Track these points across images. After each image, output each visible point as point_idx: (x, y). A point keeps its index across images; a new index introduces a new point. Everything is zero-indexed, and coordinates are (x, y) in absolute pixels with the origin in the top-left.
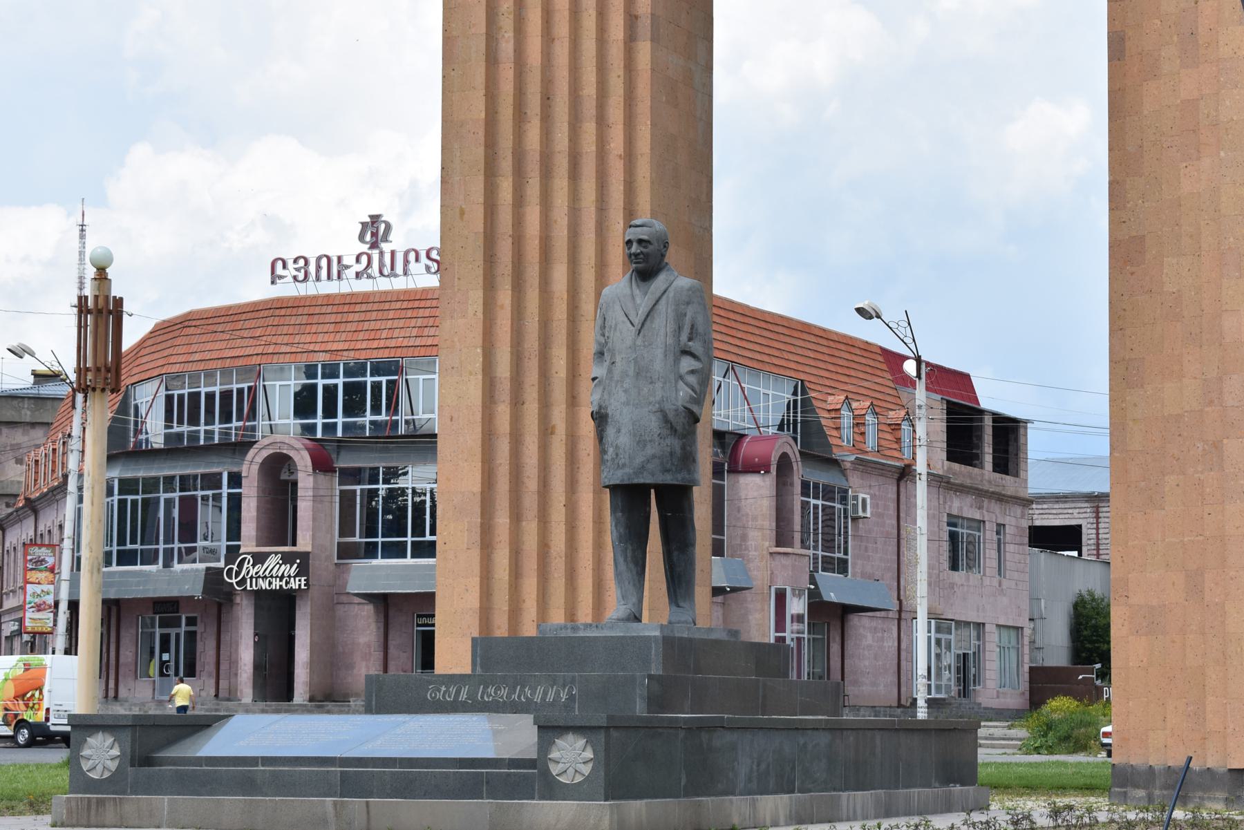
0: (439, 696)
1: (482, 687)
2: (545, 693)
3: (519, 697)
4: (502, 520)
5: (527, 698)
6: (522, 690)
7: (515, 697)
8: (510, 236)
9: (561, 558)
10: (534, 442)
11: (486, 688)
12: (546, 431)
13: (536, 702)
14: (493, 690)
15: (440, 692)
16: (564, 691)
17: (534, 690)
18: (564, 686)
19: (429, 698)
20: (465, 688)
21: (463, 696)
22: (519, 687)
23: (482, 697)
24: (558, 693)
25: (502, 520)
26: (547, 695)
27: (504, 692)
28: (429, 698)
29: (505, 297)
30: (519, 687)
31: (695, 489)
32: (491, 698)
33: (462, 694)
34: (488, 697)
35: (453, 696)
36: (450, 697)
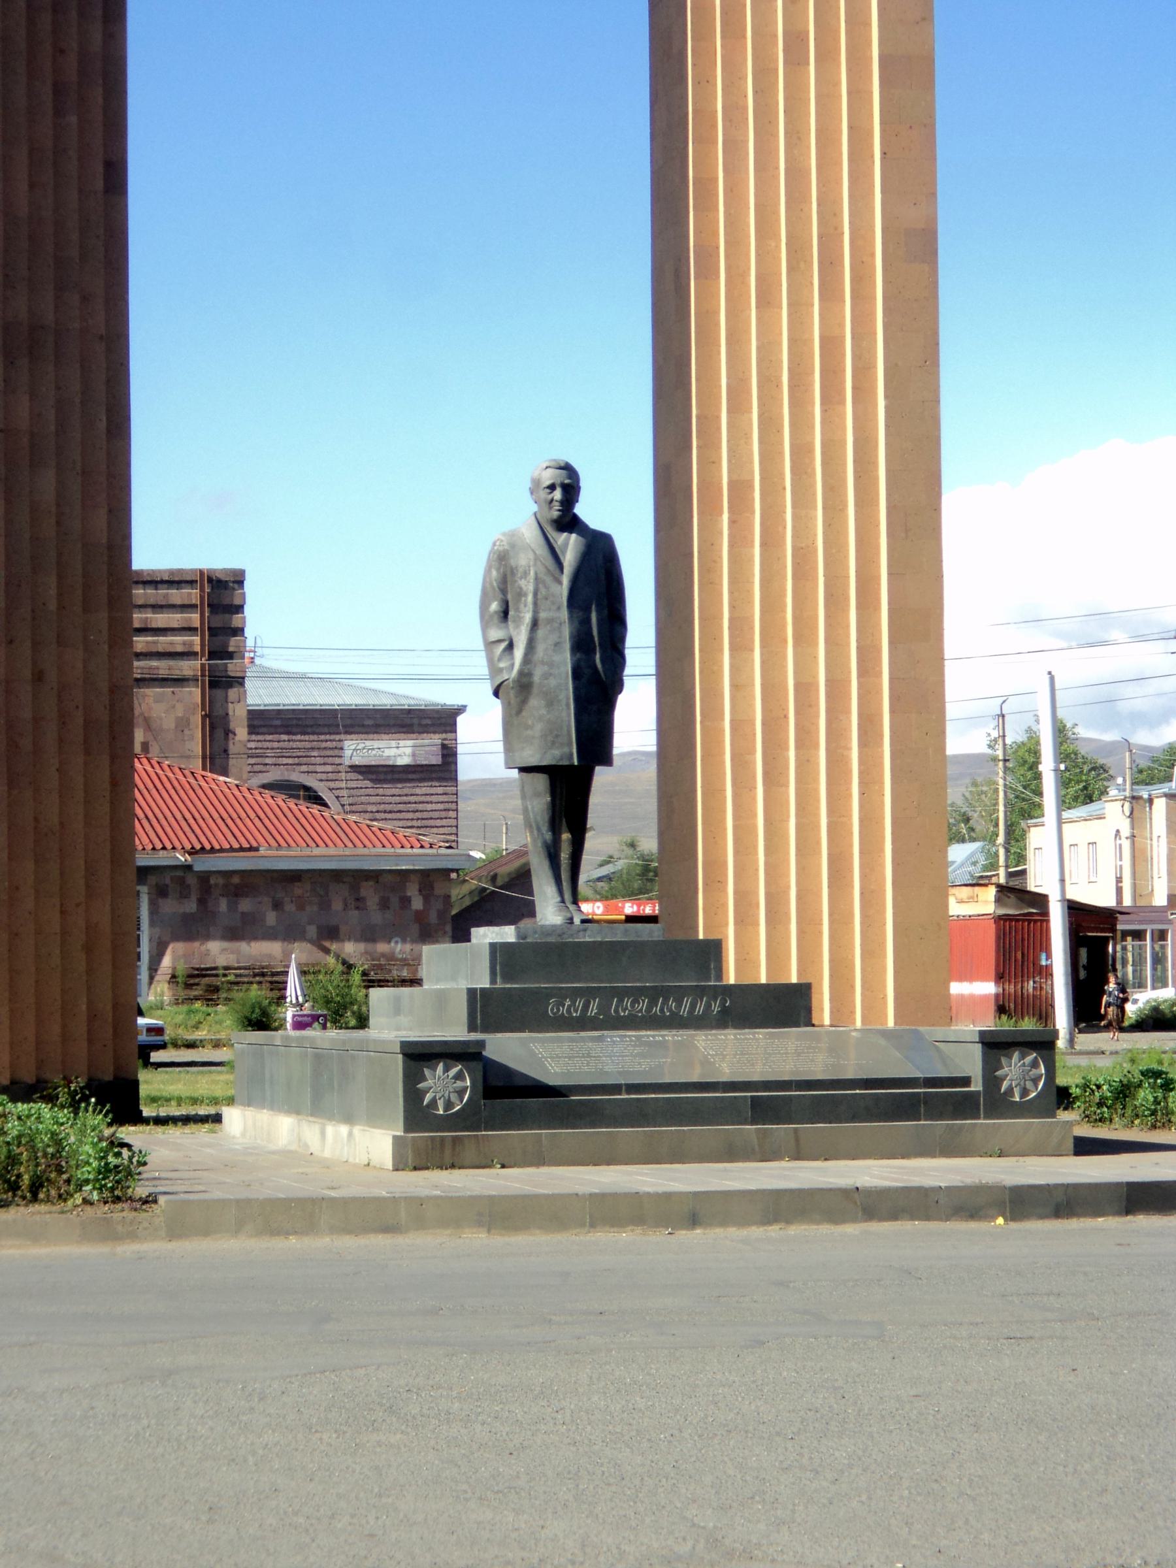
0: (563, 1010)
2: (693, 1006)
3: (662, 1010)
5: (670, 1010)
6: (666, 1000)
7: (656, 1010)
11: (621, 1001)
13: (682, 1017)
15: (563, 1008)
17: (679, 1003)
21: (593, 1010)
23: (616, 1011)
24: (708, 1006)
27: (643, 1005)
32: (627, 1012)
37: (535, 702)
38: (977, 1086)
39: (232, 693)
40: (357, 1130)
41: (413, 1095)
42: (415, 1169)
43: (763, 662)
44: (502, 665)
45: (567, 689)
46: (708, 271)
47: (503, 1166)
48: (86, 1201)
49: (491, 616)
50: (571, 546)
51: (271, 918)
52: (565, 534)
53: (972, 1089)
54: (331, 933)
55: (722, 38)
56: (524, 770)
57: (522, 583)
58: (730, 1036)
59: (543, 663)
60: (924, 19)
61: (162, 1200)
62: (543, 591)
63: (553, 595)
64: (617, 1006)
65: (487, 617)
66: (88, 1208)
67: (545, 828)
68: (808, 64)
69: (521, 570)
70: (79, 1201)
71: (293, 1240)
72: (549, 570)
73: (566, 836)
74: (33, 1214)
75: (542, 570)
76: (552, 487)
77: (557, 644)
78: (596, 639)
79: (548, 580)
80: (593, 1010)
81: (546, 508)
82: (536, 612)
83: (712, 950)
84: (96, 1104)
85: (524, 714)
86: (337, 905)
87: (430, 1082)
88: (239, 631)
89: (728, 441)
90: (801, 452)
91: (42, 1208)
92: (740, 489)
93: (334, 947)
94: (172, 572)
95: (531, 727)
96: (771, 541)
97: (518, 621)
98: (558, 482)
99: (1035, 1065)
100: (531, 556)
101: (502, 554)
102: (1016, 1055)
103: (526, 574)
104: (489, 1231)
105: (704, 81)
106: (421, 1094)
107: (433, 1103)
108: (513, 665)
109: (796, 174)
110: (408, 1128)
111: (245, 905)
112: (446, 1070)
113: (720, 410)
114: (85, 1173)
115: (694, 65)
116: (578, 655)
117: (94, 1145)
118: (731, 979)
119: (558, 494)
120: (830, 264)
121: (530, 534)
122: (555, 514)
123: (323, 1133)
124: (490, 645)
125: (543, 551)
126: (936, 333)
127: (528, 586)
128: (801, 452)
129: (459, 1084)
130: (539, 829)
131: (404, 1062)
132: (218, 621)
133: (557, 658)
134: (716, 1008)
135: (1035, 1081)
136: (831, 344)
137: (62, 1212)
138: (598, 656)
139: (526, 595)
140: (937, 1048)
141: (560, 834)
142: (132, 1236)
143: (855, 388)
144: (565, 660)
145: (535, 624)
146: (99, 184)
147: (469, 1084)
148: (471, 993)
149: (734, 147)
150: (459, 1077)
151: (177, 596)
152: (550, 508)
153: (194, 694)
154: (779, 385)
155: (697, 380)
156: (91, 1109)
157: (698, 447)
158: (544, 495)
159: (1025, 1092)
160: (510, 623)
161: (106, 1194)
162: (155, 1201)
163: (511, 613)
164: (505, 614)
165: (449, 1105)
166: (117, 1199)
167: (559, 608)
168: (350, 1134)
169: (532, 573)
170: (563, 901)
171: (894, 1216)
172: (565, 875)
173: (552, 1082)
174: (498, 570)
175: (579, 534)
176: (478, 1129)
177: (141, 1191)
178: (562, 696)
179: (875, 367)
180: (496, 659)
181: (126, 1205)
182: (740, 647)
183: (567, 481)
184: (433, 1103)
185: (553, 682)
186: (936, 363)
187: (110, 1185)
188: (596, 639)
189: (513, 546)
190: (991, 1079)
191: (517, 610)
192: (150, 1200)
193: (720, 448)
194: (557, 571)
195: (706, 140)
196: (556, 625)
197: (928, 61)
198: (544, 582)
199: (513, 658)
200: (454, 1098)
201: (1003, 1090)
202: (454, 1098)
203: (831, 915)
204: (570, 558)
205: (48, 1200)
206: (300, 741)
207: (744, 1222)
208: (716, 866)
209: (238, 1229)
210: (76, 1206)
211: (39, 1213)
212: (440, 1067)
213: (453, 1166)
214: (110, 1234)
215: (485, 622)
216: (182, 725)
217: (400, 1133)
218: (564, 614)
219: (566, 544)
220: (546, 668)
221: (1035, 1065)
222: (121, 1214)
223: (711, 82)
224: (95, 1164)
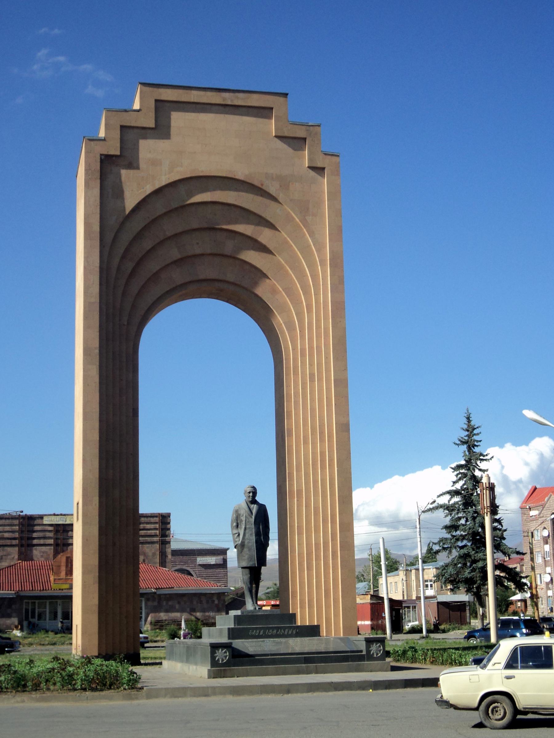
3: (280, 633)
5: (282, 633)
7: (279, 633)
11: (269, 630)
21: (261, 633)
23: (268, 633)
24: (292, 632)
27: (275, 631)
37: (246, 550)
38: (364, 653)
39: (167, 546)
40: (198, 667)
41: (213, 658)
42: (214, 678)
43: (306, 538)
44: (236, 540)
45: (254, 546)
46: (290, 435)
47: (237, 677)
48: (125, 689)
49: (234, 527)
50: (255, 508)
51: (177, 606)
52: (253, 505)
53: (363, 653)
54: (193, 610)
55: (293, 375)
56: (242, 568)
57: (242, 518)
58: (298, 640)
59: (248, 539)
60: (345, 370)
61: (145, 688)
62: (247, 520)
63: (250, 521)
64: (268, 632)
65: (233, 527)
66: (125, 691)
67: (248, 584)
68: (315, 381)
70: (122, 689)
71: (180, 699)
72: (249, 514)
73: (254, 586)
74: (110, 693)
75: (247, 514)
76: (250, 492)
77: (251, 534)
78: (262, 532)
79: (249, 517)
81: (248, 498)
82: (246, 525)
83: (294, 616)
84: (127, 662)
85: (243, 553)
86: (195, 603)
87: (218, 654)
88: (169, 529)
89: (296, 479)
90: (315, 482)
91: (113, 691)
92: (299, 492)
93: (194, 614)
94: (151, 514)
95: (245, 556)
96: (308, 506)
97: (241, 528)
98: (251, 491)
99: (380, 646)
100: (244, 511)
102: (375, 644)
103: (243, 515)
104: (233, 696)
105: (289, 386)
106: (216, 657)
107: (218, 660)
108: (240, 540)
109: (313, 410)
110: (212, 667)
111: (170, 603)
112: (222, 651)
113: (294, 471)
114: (125, 681)
115: (286, 382)
116: (257, 537)
117: (127, 673)
118: (299, 623)
119: (251, 494)
120: (322, 433)
121: (244, 505)
122: (250, 499)
123: (189, 668)
124: (234, 534)
125: (247, 509)
126: (350, 451)
127: (243, 519)
128: (315, 482)
129: (225, 654)
130: (247, 584)
131: (211, 649)
132: (164, 527)
133: (251, 538)
134: (294, 632)
135: (380, 651)
136: (323, 454)
137: (118, 692)
138: (262, 537)
139: (243, 521)
140: (354, 643)
141: (253, 585)
142: (137, 698)
143: (329, 465)
144: (254, 538)
145: (245, 529)
146: (131, 414)
147: (228, 654)
148: (229, 629)
149: (297, 403)
150: (225, 652)
151: (152, 520)
152: (249, 498)
153: (157, 546)
154: (309, 464)
155: (288, 463)
156: (125, 663)
157: (288, 481)
158: (247, 495)
159: (377, 654)
160: (239, 529)
161: (130, 687)
162: (143, 689)
163: (239, 526)
164: (237, 526)
165: (223, 660)
166: (133, 688)
167: (252, 525)
168: (196, 668)
169: (244, 515)
170: (253, 603)
171: (342, 689)
172: (254, 596)
173: (250, 653)
174: (236, 515)
175: (257, 505)
176: (230, 667)
177: (139, 685)
178: (253, 548)
179: (334, 459)
181: (135, 690)
182: (300, 533)
183: (254, 491)
184: (218, 660)
185: (250, 544)
186: (350, 458)
187: (131, 684)
188: (262, 532)
189: (239, 508)
190: (368, 651)
191: (241, 525)
192: (142, 688)
193: (294, 481)
194: (251, 515)
195: (289, 401)
196: (251, 529)
197: (346, 380)
198: (248, 518)
199: (239, 538)
200: (224, 658)
201: (371, 653)
202: (224, 658)
203: (325, 605)
204: (254, 511)
205: (114, 689)
206: (185, 558)
207: (302, 692)
208: (294, 593)
209: (165, 696)
210: (122, 690)
211: (112, 692)
212: (220, 650)
213: (224, 677)
214: (130, 698)
215: (232, 529)
216: (154, 554)
217: (210, 668)
218: (253, 526)
219: (254, 507)
220: (248, 541)
221: (380, 646)
222: (134, 692)
223: (290, 386)
224: (127, 679)
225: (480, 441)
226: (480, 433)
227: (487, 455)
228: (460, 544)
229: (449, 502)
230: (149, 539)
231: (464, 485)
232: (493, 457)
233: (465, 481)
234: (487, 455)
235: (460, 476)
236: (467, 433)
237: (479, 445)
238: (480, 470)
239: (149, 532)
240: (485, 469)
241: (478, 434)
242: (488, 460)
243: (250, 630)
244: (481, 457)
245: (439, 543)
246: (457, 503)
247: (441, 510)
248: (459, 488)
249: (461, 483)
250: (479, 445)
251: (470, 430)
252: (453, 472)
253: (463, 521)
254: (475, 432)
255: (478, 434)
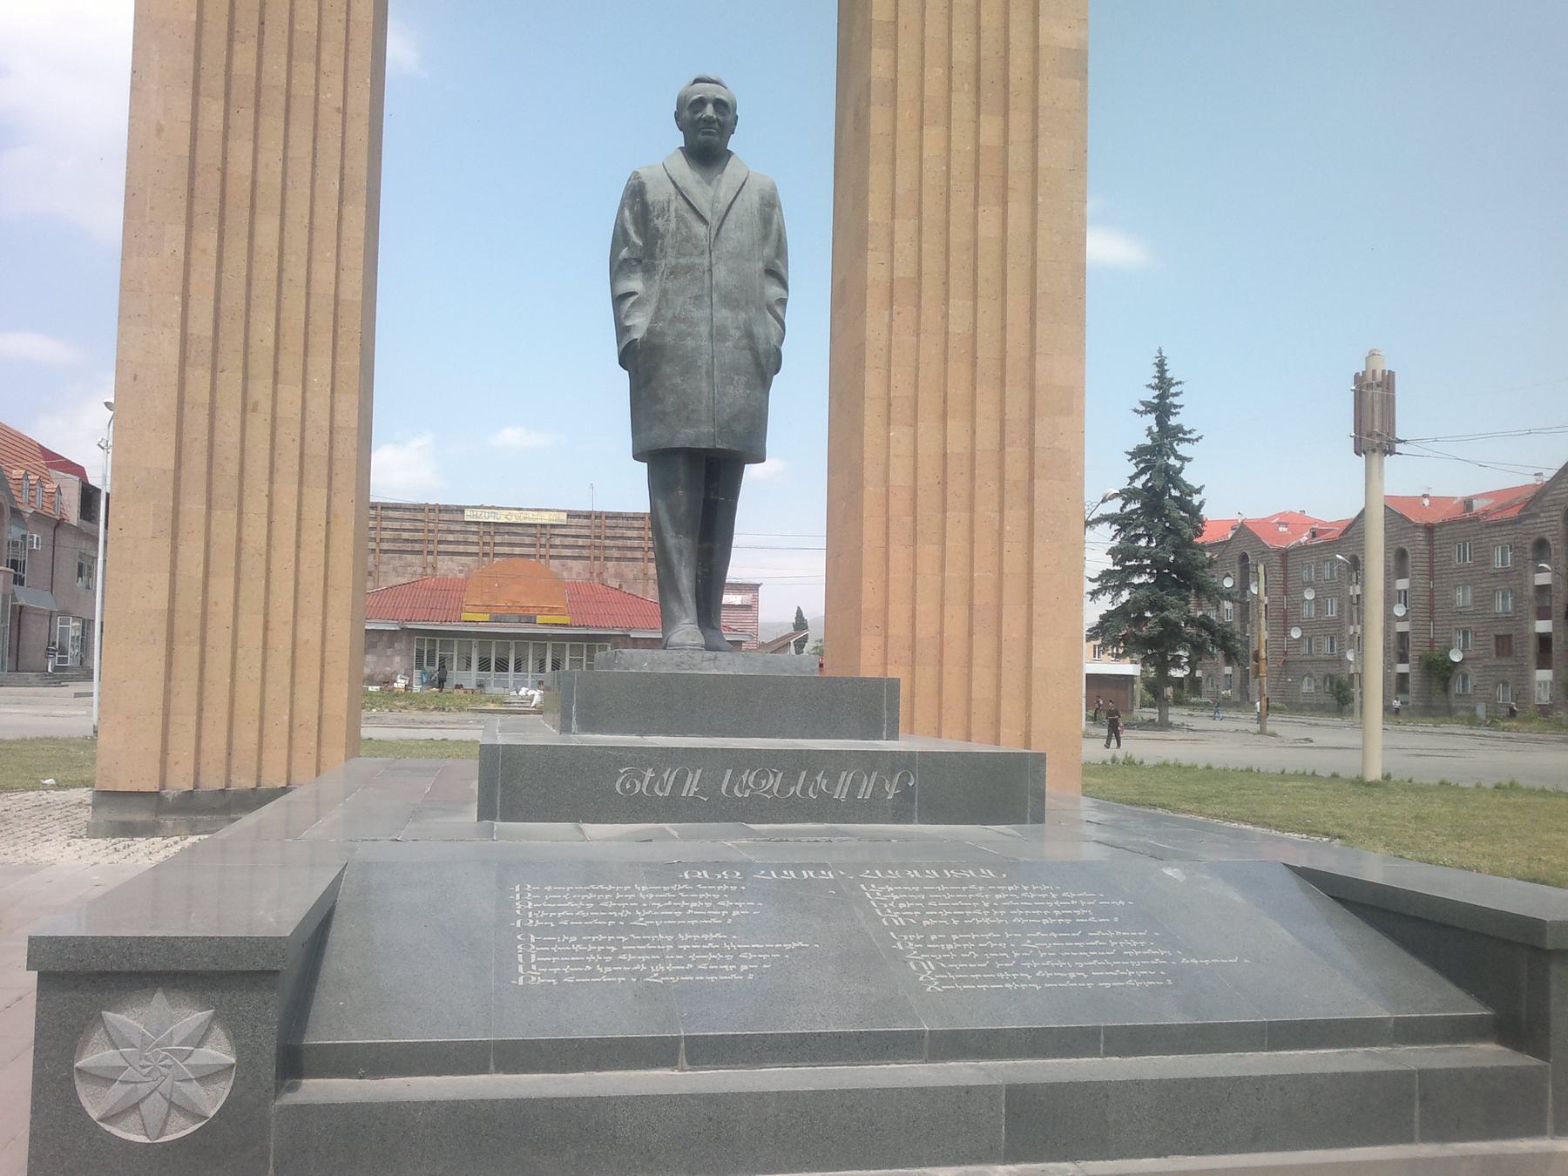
0: (641, 787)
1: (729, 772)
2: (855, 784)
3: (804, 790)
4: (194, 506)
6: (811, 778)
8: (218, 169)
9: (261, 555)
10: (235, 417)
11: (737, 773)
12: (246, 408)
14: (752, 778)
15: (642, 782)
16: (891, 781)
17: (833, 778)
18: (893, 772)
19: (618, 790)
20: (694, 773)
21: (691, 787)
22: (804, 774)
23: (730, 790)
24: (880, 786)
25: (194, 506)
26: (859, 788)
27: (773, 782)
28: (618, 790)
29: (207, 240)
30: (804, 774)
31: (751, 472)
33: (688, 784)
34: (741, 791)
35: (669, 788)
36: (662, 789)
57: (659, 223)
69: (658, 207)
80: (691, 787)
101: (637, 189)
126: (1084, 140)
134: (891, 791)
180: (623, 316)
225: (1181, 406)
226: (1181, 392)
227: (1190, 432)
228: (1136, 581)
229: (1122, 510)
230: (629, 554)
231: (1148, 481)
232: (1201, 437)
233: (1151, 474)
234: (1190, 432)
235: (1142, 465)
236: (1157, 392)
237: (1178, 413)
238: (1178, 457)
239: (629, 543)
240: (1188, 456)
241: (1176, 394)
242: (1193, 440)
243: (621, 763)
244: (1181, 435)
245: (1099, 578)
246: (1134, 511)
247: (1107, 524)
248: (1140, 487)
249: (1144, 478)
250: (1178, 413)
251: (1165, 386)
252: (1129, 460)
253: (1143, 542)
254: (1173, 390)
255: (1176, 394)
